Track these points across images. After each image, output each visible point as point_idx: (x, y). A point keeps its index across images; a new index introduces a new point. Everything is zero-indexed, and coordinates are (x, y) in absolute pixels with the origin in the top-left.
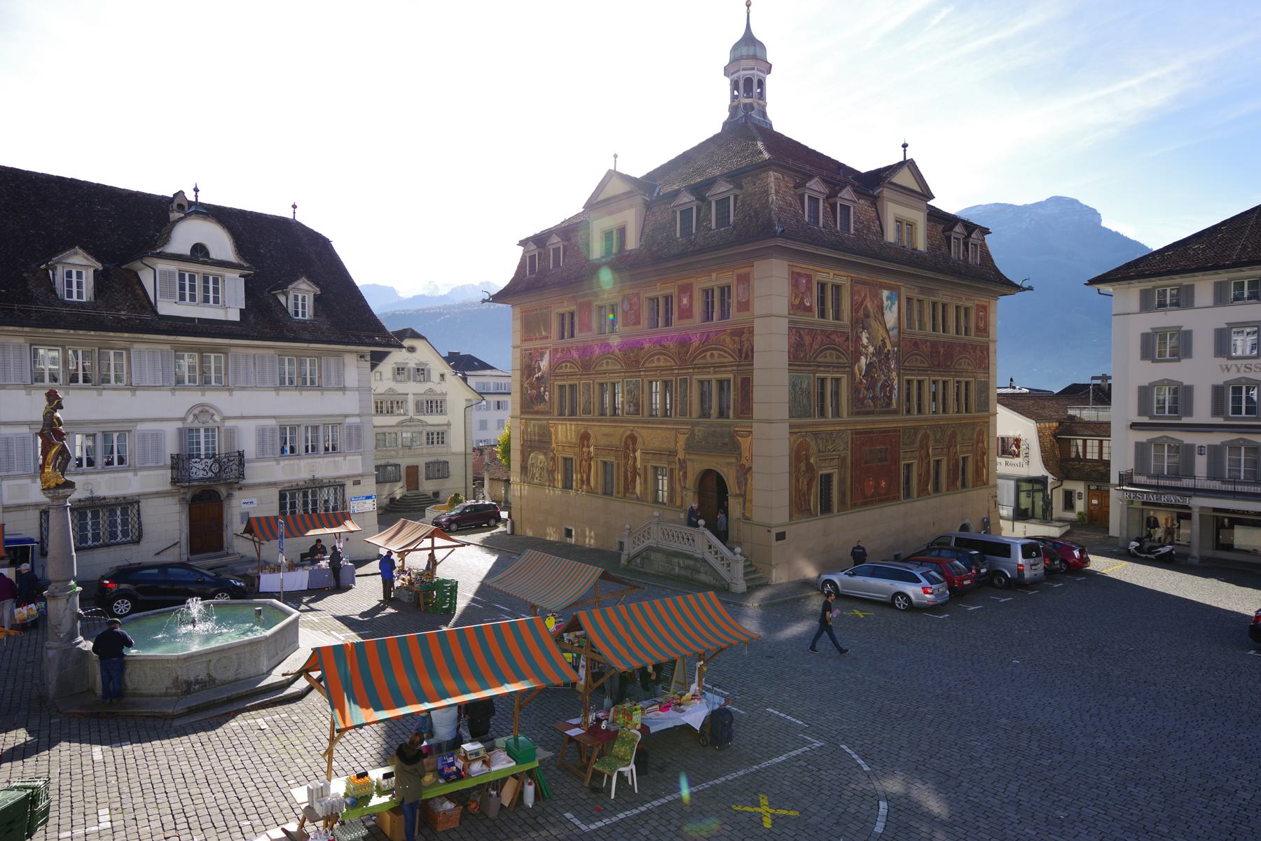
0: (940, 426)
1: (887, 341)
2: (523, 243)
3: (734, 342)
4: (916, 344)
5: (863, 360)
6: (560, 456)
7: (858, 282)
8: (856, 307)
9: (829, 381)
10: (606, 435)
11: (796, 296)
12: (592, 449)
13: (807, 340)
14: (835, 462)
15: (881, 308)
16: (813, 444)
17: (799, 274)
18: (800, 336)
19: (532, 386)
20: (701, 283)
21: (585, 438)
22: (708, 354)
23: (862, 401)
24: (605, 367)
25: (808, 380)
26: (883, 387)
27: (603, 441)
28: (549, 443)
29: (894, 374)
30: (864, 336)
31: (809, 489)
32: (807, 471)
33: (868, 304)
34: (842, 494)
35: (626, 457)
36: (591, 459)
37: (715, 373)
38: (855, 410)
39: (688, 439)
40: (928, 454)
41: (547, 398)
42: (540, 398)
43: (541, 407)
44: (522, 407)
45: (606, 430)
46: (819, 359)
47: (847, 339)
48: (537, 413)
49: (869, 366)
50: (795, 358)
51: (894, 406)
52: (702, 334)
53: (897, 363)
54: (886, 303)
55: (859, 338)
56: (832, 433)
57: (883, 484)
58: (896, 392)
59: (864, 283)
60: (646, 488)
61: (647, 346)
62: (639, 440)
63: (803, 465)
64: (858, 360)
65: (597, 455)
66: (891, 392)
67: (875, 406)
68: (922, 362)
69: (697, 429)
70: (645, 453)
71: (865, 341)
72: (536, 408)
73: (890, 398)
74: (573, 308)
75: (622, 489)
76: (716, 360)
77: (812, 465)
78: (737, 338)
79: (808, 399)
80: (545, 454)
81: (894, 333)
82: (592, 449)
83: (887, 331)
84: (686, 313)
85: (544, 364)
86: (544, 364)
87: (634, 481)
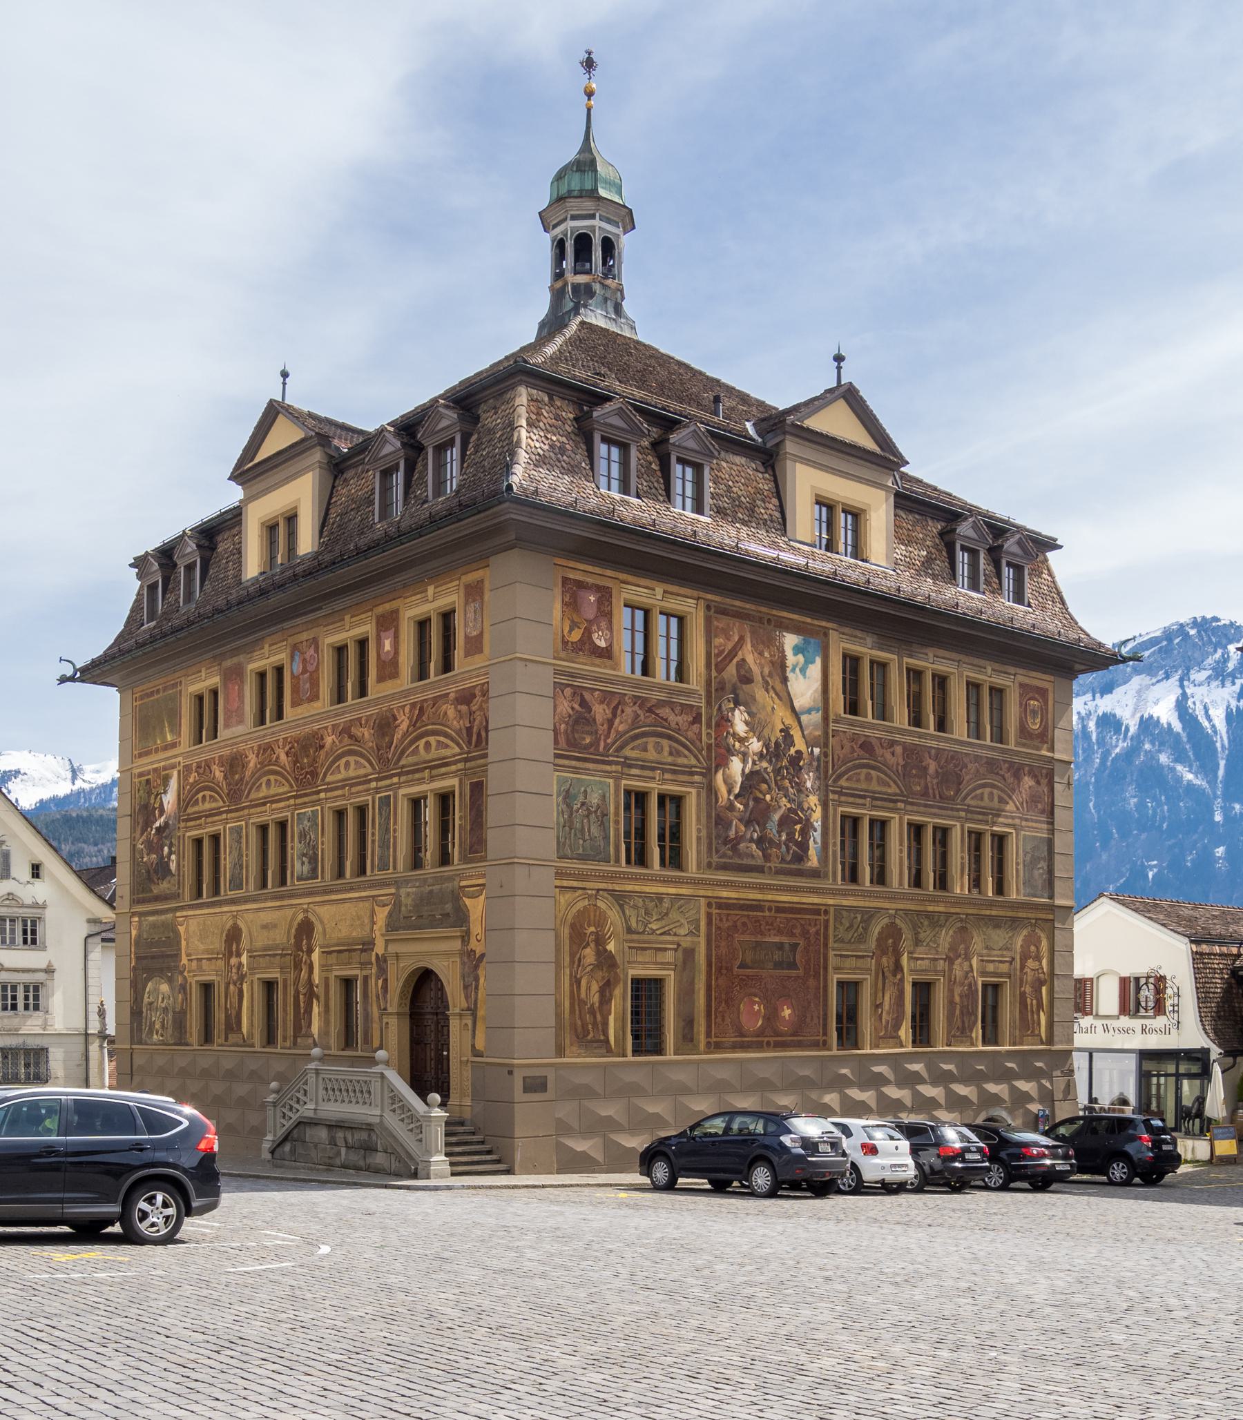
1: (796, 733)
2: (140, 563)
3: (460, 715)
6: (194, 980)
8: (716, 662)
10: (265, 927)
13: (600, 712)
14: (668, 956)
15: (780, 667)
16: (613, 915)
18: (583, 703)
20: (413, 609)
21: (234, 936)
22: (422, 742)
24: (264, 792)
26: (785, 822)
27: (262, 940)
28: (177, 956)
29: (813, 800)
31: (605, 1000)
32: (598, 966)
34: (687, 1023)
35: (297, 966)
36: (242, 978)
37: (433, 778)
38: (715, 859)
39: (390, 915)
41: (173, 866)
42: (162, 869)
43: (164, 886)
44: (132, 893)
45: (266, 917)
46: (627, 752)
47: (697, 719)
48: (157, 899)
49: (752, 779)
50: (572, 744)
52: (413, 705)
53: (822, 775)
54: (791, 659)
55: (724, 721)
56: (660, 898)
57: (787, 1012)
58: (817, 835)
59: (723, 612)
60: (327, 1022)
61: (329, 740)
62: (318, 928)
63: (589, 954)
66: (805, 832)
67: (767, 857)
68: (879, 780)
69: (403, 891)
71: (740, 728)
73: (804, 846)
74: (215, 680)
75: (290, 1032)
76: (434, 754)
77: (610, 956)
78: (464, 708)
79: (603, 825)
80: (170, 981)
82: (244, 959)
83: (796, 714)
84: (389, 669)
85: (169, 800)
86: (169, 800)
87: (309, 1011)
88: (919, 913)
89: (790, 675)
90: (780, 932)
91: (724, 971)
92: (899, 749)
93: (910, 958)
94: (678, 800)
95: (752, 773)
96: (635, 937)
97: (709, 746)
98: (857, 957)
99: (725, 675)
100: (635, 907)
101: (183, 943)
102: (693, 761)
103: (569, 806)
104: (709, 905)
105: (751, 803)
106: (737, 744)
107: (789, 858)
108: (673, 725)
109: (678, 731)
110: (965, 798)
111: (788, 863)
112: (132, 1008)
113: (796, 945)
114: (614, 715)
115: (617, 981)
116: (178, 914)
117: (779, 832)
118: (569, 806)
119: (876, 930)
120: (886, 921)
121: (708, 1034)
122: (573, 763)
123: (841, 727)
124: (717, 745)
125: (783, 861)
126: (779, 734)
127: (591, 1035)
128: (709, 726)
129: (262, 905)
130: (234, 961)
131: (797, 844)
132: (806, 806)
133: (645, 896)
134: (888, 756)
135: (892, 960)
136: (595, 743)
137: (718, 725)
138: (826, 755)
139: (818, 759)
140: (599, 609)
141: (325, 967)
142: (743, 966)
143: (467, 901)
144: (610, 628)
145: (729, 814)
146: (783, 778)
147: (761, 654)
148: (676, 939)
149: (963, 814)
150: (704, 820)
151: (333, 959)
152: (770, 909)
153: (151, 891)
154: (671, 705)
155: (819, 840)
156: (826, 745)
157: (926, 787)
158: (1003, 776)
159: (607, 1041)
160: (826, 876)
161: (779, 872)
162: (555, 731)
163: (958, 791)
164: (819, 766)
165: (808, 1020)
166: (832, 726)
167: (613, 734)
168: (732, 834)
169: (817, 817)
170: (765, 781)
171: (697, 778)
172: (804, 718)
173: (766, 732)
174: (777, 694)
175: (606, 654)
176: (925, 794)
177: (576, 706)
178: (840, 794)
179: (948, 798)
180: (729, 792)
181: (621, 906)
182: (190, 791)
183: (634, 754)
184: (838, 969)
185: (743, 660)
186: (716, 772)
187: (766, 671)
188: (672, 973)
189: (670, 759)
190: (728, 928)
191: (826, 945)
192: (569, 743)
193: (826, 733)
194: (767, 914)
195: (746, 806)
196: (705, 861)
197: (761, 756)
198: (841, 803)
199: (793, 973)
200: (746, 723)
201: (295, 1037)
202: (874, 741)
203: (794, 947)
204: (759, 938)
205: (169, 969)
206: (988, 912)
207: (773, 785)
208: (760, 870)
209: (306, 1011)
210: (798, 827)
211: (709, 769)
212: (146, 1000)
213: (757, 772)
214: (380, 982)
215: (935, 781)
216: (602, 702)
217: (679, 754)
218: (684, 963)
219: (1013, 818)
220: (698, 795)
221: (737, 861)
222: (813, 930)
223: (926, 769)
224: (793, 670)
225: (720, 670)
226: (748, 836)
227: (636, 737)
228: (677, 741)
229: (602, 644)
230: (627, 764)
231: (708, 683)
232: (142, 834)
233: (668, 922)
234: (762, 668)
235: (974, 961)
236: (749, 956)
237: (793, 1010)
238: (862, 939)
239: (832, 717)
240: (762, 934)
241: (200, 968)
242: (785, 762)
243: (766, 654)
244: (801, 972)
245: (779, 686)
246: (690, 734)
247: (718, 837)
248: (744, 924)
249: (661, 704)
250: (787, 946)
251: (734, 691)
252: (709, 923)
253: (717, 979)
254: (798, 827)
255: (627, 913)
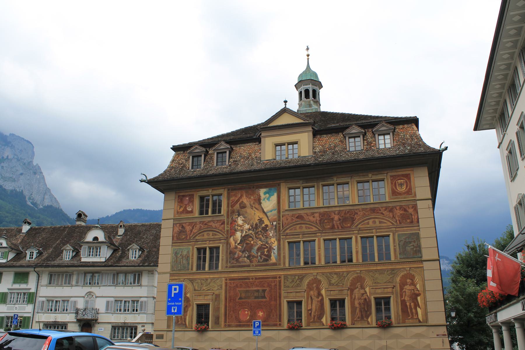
0: (336, 273)
4: (300, 217)
5: (238, 235)
7: (233, 190)
9: (208, 249)
11: (181, 207)
13: (188, 228)
14: (210, 297)
16: (190, 286)
17: (184, 196)
18: (183, 227)
23: (237, 260)
25: (190, 250)
26: (258, 250)
29: (273, 240)
30: (240, 221)
33: (245, 200)
38: (229, 265)
40: (319, 294)
46: (197, 238)
47: (223, 223)
51: (273, 259)
54: (262, 196)
55: (234, 221)
56: (207, 279)
58: (276, 251)
64: (232, 233)
67: (251, 262)
77: (188, 298)
81: (273, 214)
88: (331, 273)
89: (262, 201)
90: (257, 286)
91: (232, 301)
92: (317, 215)
93: (327, 290)
94: (218, 248)
95: (245, 236)
96: (197, 292)
97: (227, 231)
98: (296, 292)
99: (235, 208)
100: (197, 283)
102: (221, 236)
103: (176, 256)
104: (226, 280)
105: (245, 245)
106: (239, 228)
107: (261, 261)
108: (214, 227)
109: (216, 228)
110: (357, 225)
111: (262, 262)
113: (265, 290)
114: (193, 228)
115: (190, 305)
117: (257, 253)
118: (176, 256)
119: (306, 282)
120: (312, 277)
121: (225, 322)
122: (178, 244)
123: (287, 213)
124: (231, 230)
125: (259, 262)
126: (257, 221)
127: (180, 322)
128: (228, 224)
131: (265, 255)
132: (269, 242)
133: (201, 279)
134: (311, 218)
135: (317, 292)
136: (187, 237)
137: (231, 223)
138: (279, 224)
139: (276, 226)
140: (189, 201)
142: (240, 298)
144: (193, 205)
145: (235, 250)
146: (259, 235)
147: (250, 198)
148: (213, 291)
149: (357, 232)
150: (225, 253)
152: (252, 279)
154: (213, 221)
155: (276, 253)
156: (279, 220)
157: (333, 225)
158: (382, 213)
159: (186, 324)
160: (280, 264)
161: (256, 266)
162: (173, 236)
163: (352, 223)
164: (275, 229)
165: (271, 316)
166: (282, 214)
167: (192, 233)
168: (236, 256)
169: (275, 246)
170: (251, 237)
171: (222, 241)
172: (268, 214)
173: (251, 222)
174: (256, 209)
175: (192, 212)
176: (333, 227)
177: (180, 228)
178: (287, 235)
179: (348, 227)
180: (235, 243)
181: (193, 283)
183: (199, 238)
184: (285, 297)
185: (242, 202)
186: (230, 237)
187: (252, 203)
188: (211, 302)
189: (212, 237)
190: (234, 287)
191: (280, 289)
192: (177, 239)
193: (279, 217)
194: (251, 280)
195: (242, 246)
196: (225, 265)
197: (249, 229)
198: (287, 239)
199: (264, 300)
200: (243, 220)
202: (303, 215)
203: (264, 291)
204: (248, 289)
206: (375, 268)
207: (254, 238)
208: (249, 266)
210: (266, 250)
211: (227, 238)
213: (247, 235)
215: (338, 222)
216: (189, 225)
217: (216, 235)
218: (216, 298)
219: (391, 228)
220: (223, 246)
221: (238, 264)
222: (273, 284)
223: (333, 219)
224: (264, 199)
225: (232, 206)
226: (243, 256)
227: (199, 233)
228: (215, 231)
229: (190, 210)
230: (197, 241)
231: (228, 212)
233: (211, 287)
234: (250, 202)
235: (367, 290)
236: (243, 295)
237: (264, 312)
238: (298, 285)
239: (282, 210)
240: (249, 287)
242: (260, 229)
243: (252, 198)
244: (268, 299)
245: (257, 206)
246: (220, 228)
247: (230, 258)
248: (241, 285)
249: (209, 222)
250: (261, 291)
251: (238, 212)
252: (226, 285)
253: (229, 303)
254: (266, 250)
255: (194, 285)
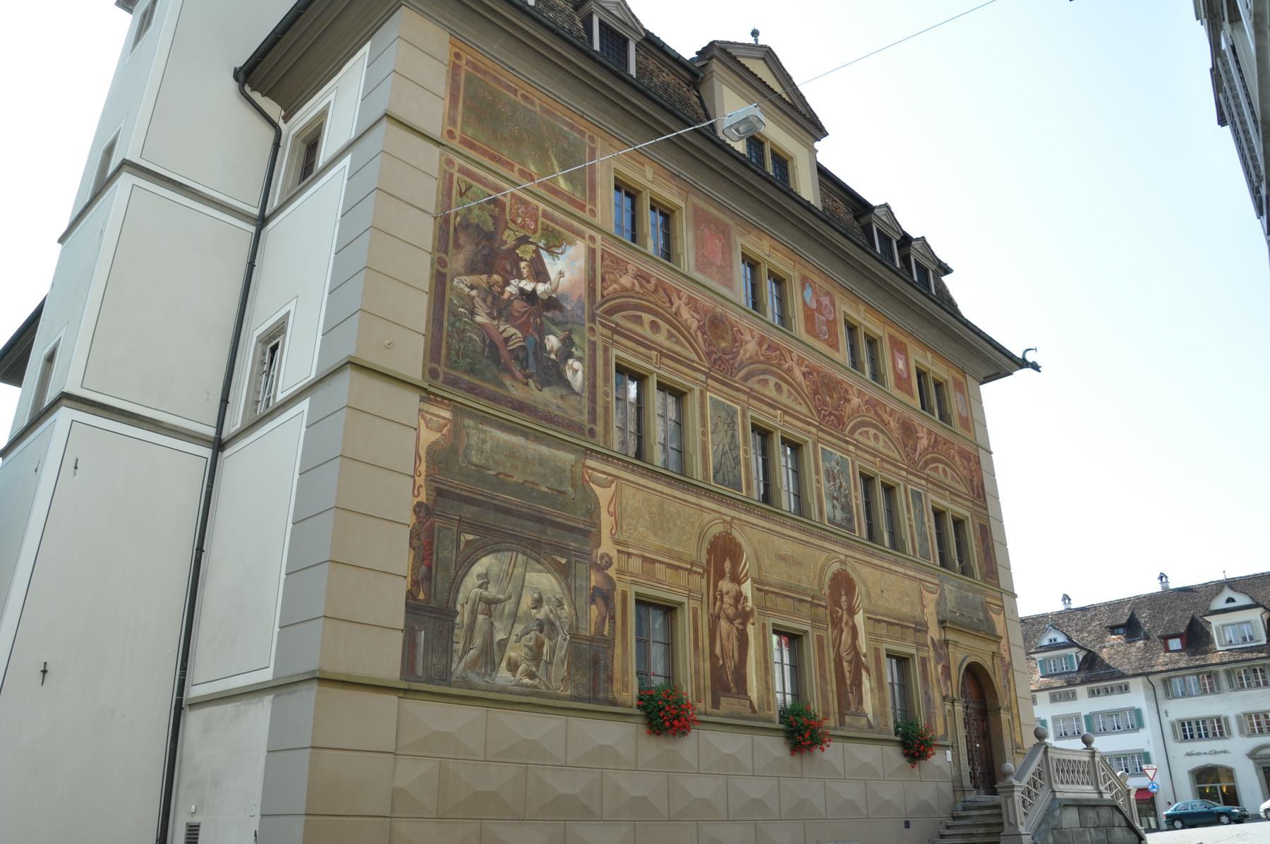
6: (628, 589)
12: (747, 588)
19: (500, 308)
27: (777, 574)
28: (589, 532)
35: (836, 623)
36: (745, 616)
45: (788, 548)
60: (882, 702)
62: (860, 588)
65: (763, 608)
70: (872, 620)
72: (517, 391)
80: (564, 573)
101: (606, 521)
112: (411, 595)
116: (590, 463)
129: (778, 529)
130: (725, 585)
141: (873, 637)
143: (993, 616)
151: (882, 630)
153: (501, 384)
182: (615, 291)
201: (842, 715)
205: (563, 551)
209: (853, 684)
212: (470, 586)
214: (940, 668)
232: (472, 269)
241: (651, 575)
